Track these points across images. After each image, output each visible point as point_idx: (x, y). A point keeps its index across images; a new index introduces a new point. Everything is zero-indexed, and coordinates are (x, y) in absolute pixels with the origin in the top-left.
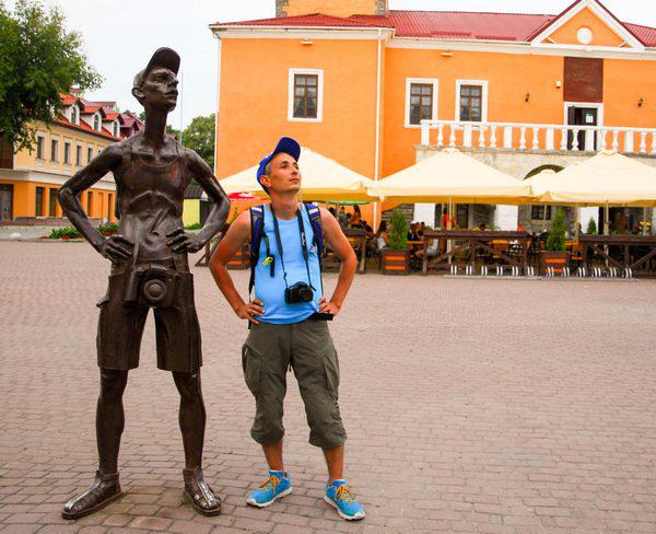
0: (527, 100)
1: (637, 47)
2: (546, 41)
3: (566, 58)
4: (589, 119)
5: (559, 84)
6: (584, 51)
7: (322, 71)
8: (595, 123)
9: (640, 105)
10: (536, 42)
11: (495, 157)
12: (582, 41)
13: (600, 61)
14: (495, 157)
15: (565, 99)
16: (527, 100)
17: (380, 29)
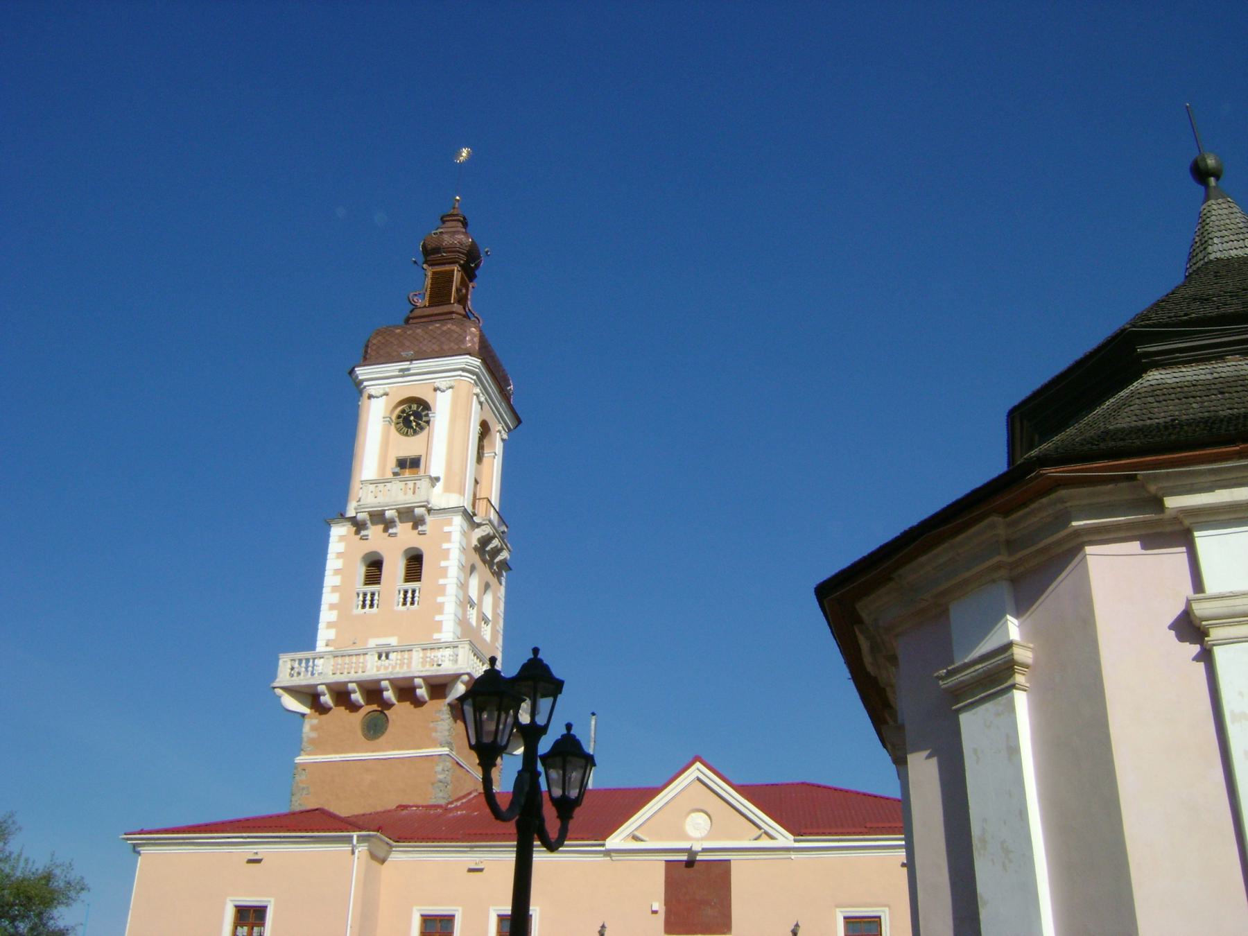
1: (784, 838)
2: (636, 838)
5: (658, 905)
7: (272, 900)
10: (616, 841)
13: (729, 861)
17: (355, 835)
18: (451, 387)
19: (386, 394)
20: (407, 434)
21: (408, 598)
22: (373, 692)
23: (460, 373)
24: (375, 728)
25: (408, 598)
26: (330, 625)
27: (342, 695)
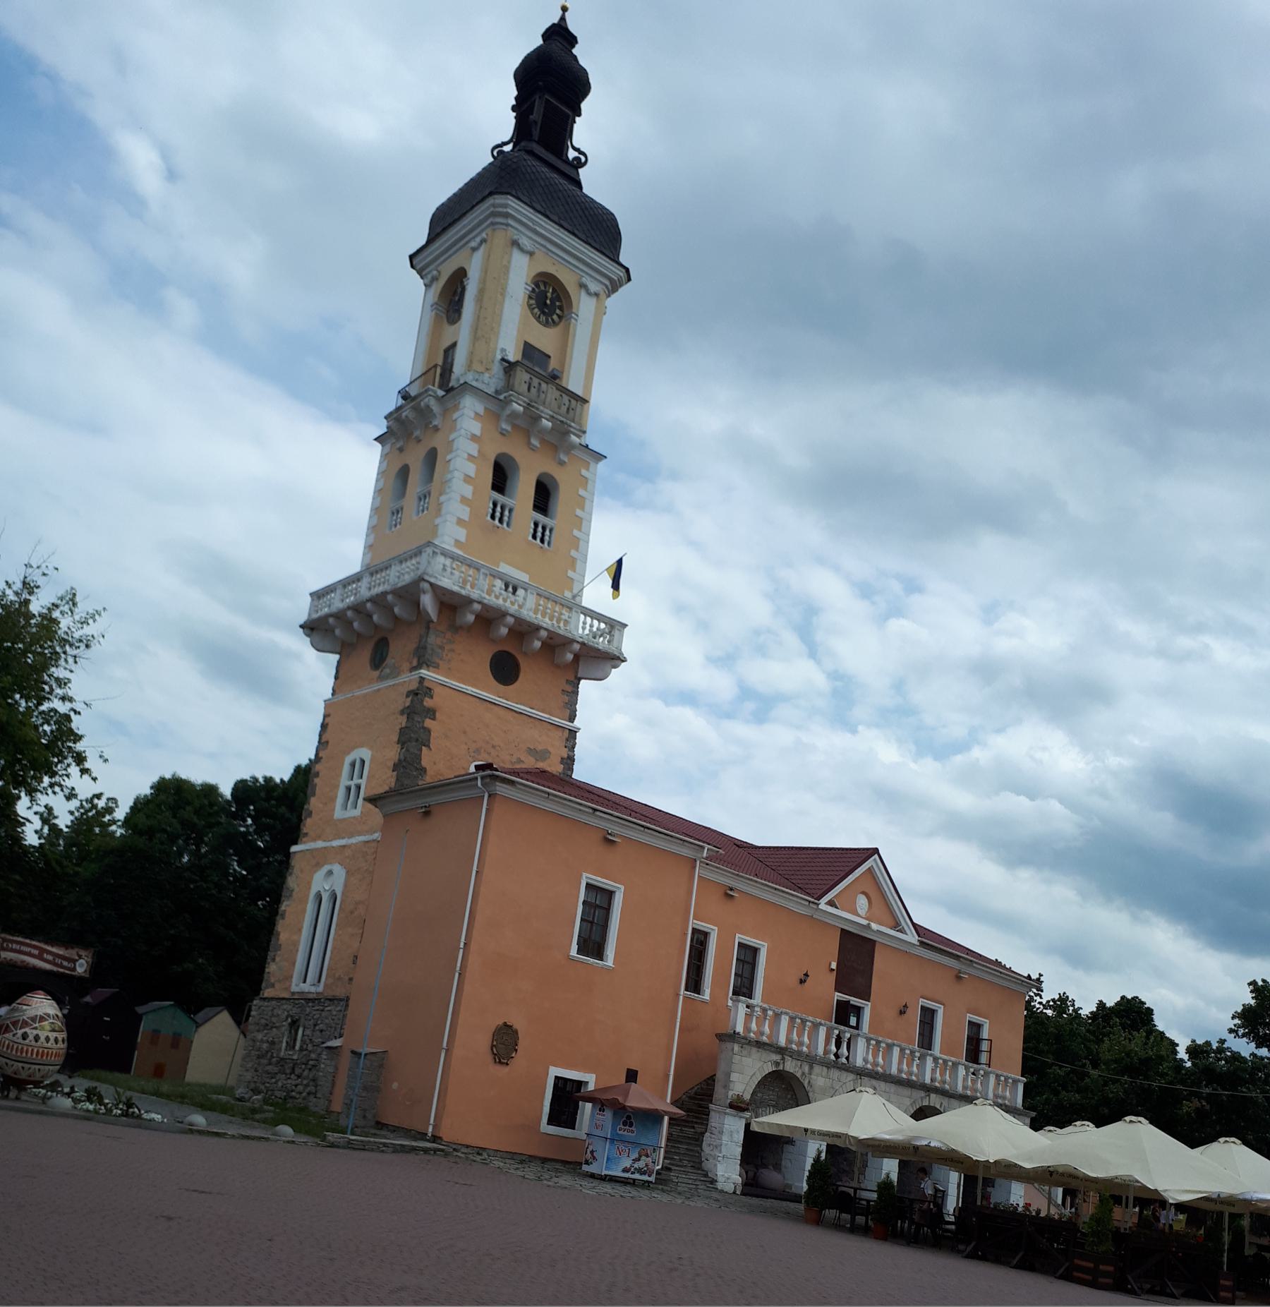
0: (802, 982)
1: (912, 938)
2: (831, 903)
3: (844, 932)
4: (853, 1021)
5: (834, 966)
6: (868, 927)
7: (622, 888)
8: (857, 1028)
9: (902, 1013)
10: (823, 904)
11: (811, 1068)
12: (860, 911)
14: (811, 1068)
15: (837, 990)
16: (802, 982)
17: (707, 846)
18: (597, 295)
19: (531, 254)
20: (538, 319)
21: (540, 533)
22: (524, 631)
23: (608, 283)
24: (505, 670)
25: (540, 533)
26: (460, 522)
27: (489, 618)
